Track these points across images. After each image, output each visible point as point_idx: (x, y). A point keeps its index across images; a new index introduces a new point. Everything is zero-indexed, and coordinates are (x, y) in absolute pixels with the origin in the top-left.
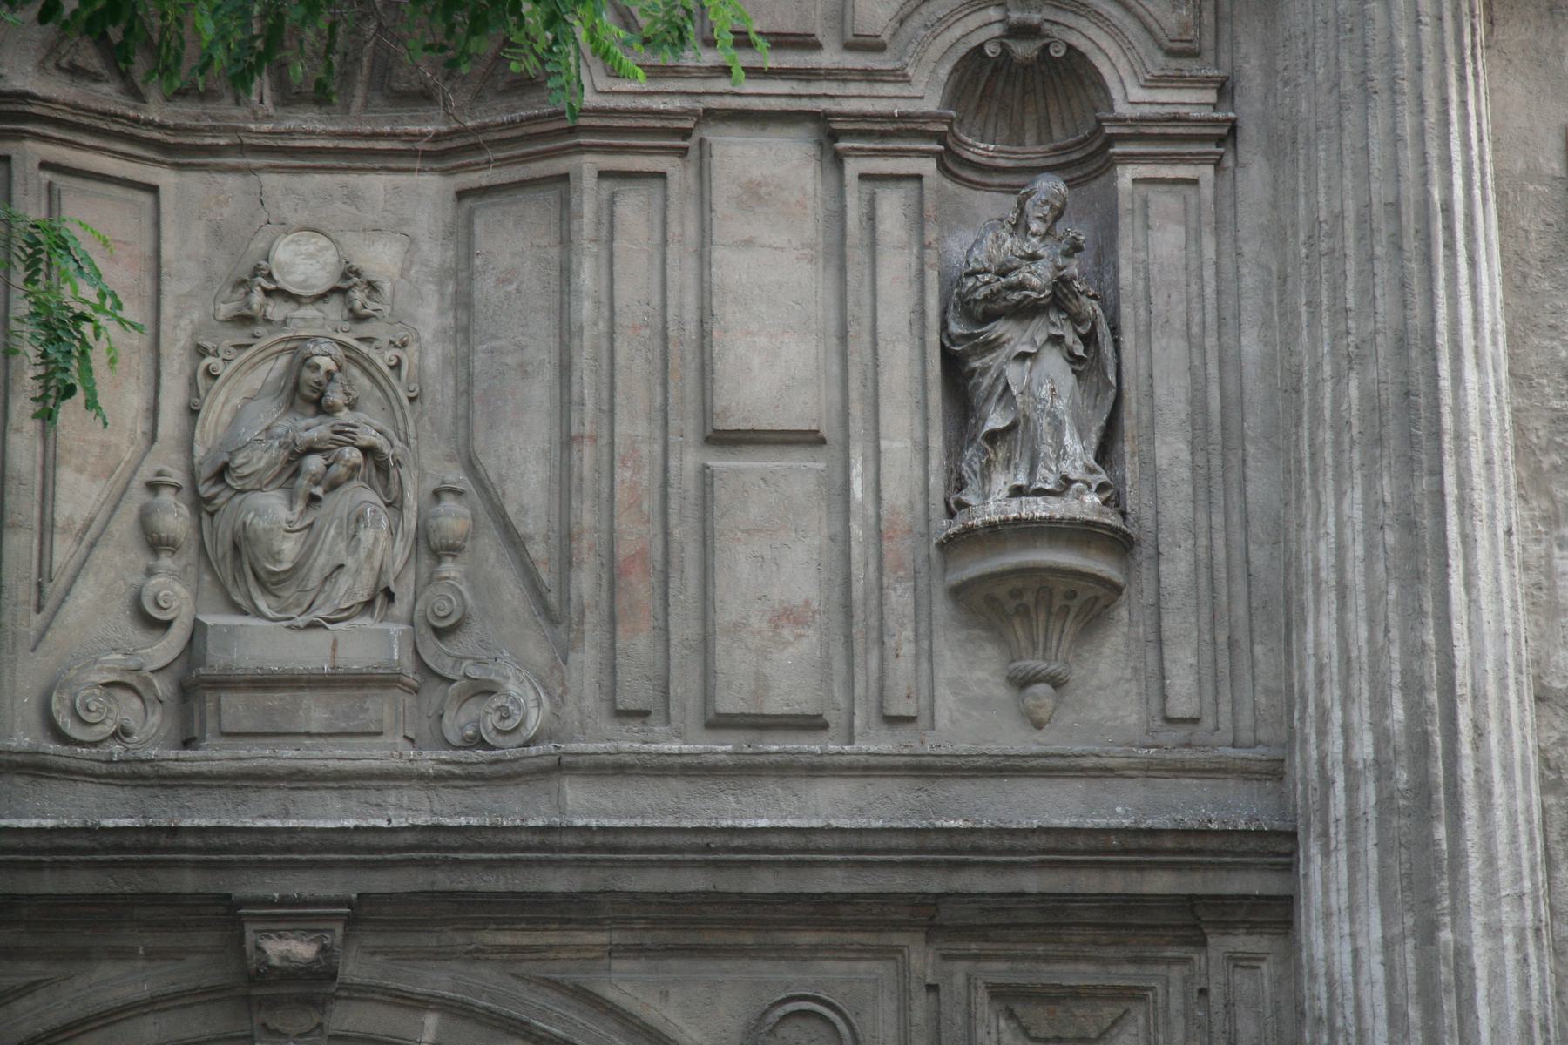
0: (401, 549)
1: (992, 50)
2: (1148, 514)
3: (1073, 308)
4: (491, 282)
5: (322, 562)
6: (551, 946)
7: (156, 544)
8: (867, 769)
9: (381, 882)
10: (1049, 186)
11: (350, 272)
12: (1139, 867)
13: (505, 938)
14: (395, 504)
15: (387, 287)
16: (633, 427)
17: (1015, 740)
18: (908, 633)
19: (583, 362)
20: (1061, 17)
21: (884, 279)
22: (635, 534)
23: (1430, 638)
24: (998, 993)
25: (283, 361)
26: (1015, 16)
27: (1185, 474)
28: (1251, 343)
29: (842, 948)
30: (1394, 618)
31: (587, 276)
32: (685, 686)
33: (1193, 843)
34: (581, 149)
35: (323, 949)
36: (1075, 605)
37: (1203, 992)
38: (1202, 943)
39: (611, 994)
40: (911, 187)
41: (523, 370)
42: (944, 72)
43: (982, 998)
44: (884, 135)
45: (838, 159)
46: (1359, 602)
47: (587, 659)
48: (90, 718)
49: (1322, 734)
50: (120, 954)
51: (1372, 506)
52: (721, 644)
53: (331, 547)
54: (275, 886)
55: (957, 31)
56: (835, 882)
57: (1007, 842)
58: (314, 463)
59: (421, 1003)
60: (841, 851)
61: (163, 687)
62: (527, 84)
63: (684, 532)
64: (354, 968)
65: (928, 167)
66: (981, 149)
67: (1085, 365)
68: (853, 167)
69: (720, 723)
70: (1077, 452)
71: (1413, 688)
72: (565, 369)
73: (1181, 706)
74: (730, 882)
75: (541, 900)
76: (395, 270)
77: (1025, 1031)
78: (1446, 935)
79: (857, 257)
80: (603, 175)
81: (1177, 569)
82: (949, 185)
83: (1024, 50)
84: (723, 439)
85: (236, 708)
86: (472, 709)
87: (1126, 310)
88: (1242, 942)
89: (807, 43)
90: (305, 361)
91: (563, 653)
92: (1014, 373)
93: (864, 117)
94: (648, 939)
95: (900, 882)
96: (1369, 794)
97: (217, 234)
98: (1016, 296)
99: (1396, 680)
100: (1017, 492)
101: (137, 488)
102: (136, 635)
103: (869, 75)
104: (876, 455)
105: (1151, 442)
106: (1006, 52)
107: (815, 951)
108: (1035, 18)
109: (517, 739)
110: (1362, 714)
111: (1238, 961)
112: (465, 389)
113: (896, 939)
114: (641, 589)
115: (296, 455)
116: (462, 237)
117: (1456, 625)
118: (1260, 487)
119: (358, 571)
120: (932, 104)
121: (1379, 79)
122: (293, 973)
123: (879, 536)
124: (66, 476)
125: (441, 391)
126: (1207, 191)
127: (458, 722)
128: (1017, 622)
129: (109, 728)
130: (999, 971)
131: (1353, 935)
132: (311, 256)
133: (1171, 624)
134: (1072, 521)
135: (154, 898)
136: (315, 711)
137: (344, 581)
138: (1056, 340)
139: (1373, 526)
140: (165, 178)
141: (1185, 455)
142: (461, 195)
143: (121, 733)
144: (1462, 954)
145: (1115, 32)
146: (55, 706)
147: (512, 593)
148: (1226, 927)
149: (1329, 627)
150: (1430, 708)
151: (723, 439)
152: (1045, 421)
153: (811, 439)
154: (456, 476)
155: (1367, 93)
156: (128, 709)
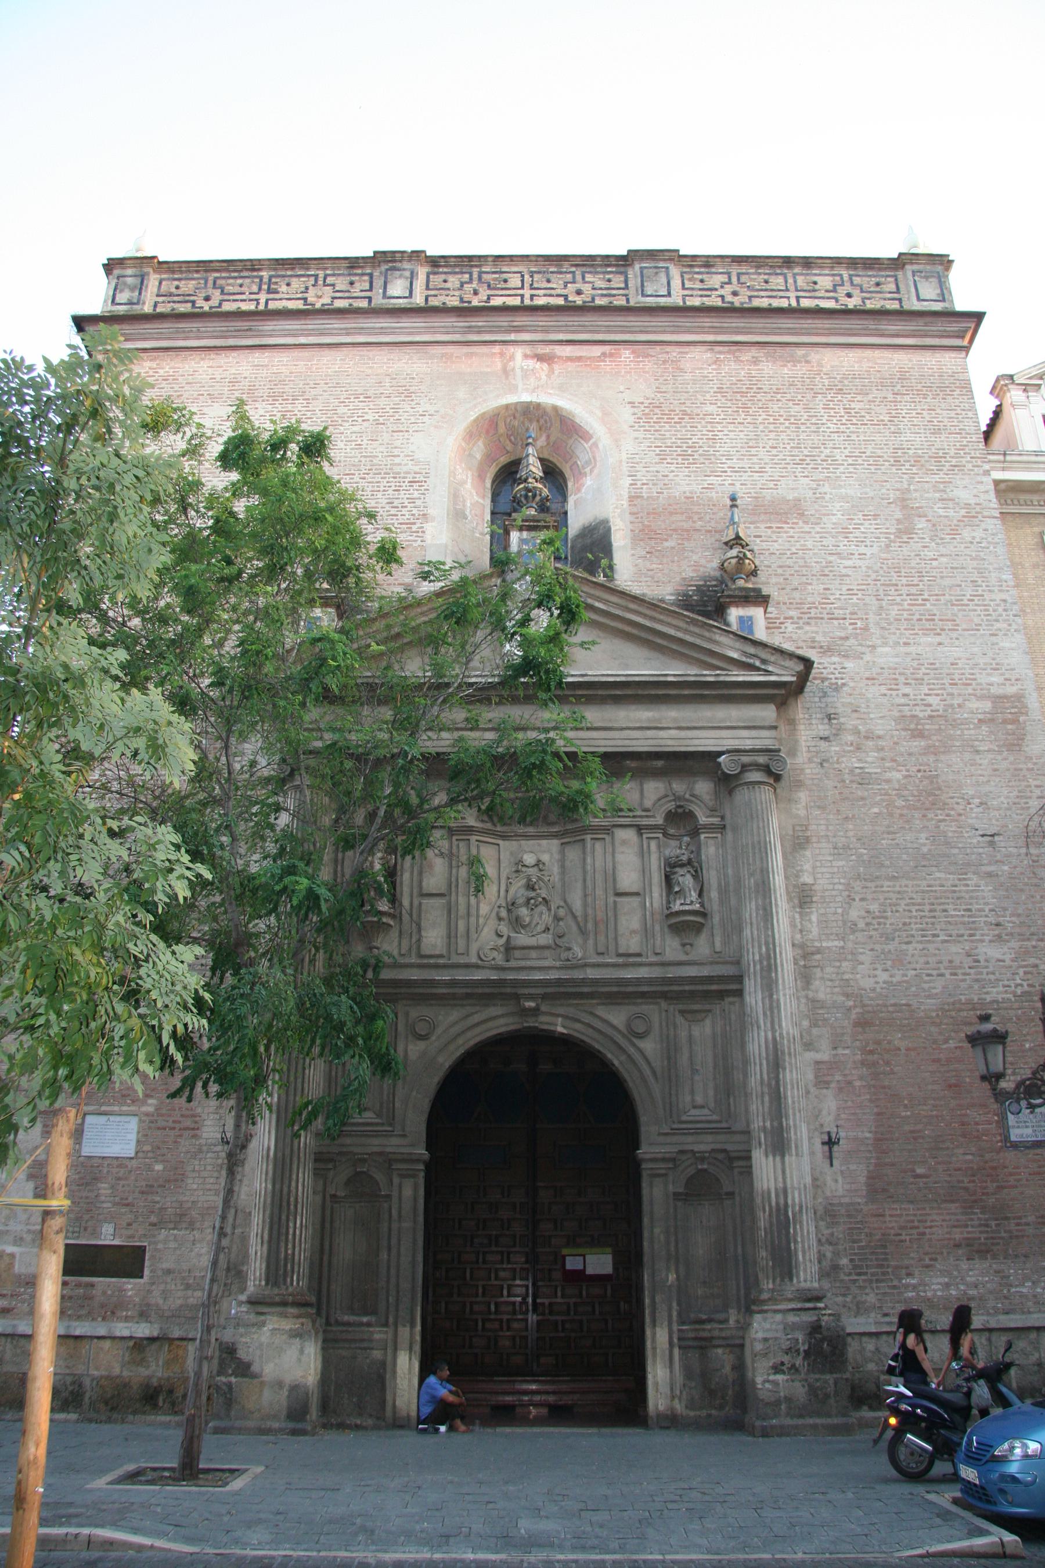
7: (500, 919)
8: (651, 964)
9: (549, 990)
10: (686, 839)
14: (549, 910)
16: (599, 892)
17: (683, 958)
19: (588, 878)
22: (600, 915)
31: (589, 860)
32: (612, 948)
47: (591, 942)
53: (536, 919)
54: (526, 991)
56: (645, 989)
59: (558, 1015)
63: (610, 914)
64: (543, 1008)
66: (672, 831)
69: (619, 955)
70: (694, 895)
71: (767, 944)
72: (585, 880)
74: (623, 989)
79: (646, 855)
81: (716, 920)
83: (680, 810)
85: (517, 954)
88: (731, 999)
90: (529, 880)
91: (585, 941)
92: (680, 879)
96: (758, 967)
97: (512, 854)
102: (495, 937)
104: (651, 897)
110: (756, 950)
111: (731, 1003)
112: (563, 885)
114: (602, 927)
115: (529, 900)
116: (562, 853)
118: (733, 902)
122: (530, 1009)
123: (652, 914)
124: (482, 905)
125: (558, 885)
127: (564, 955)
130: (681, 1007)
135: (501, 994)
136: (534, 954)
139: (757, 909)
140: (500, 842)
144: (778, 1000)
147: (574, 928)
153: (637, 894)
154: (562, 904)
156: (495, 954)
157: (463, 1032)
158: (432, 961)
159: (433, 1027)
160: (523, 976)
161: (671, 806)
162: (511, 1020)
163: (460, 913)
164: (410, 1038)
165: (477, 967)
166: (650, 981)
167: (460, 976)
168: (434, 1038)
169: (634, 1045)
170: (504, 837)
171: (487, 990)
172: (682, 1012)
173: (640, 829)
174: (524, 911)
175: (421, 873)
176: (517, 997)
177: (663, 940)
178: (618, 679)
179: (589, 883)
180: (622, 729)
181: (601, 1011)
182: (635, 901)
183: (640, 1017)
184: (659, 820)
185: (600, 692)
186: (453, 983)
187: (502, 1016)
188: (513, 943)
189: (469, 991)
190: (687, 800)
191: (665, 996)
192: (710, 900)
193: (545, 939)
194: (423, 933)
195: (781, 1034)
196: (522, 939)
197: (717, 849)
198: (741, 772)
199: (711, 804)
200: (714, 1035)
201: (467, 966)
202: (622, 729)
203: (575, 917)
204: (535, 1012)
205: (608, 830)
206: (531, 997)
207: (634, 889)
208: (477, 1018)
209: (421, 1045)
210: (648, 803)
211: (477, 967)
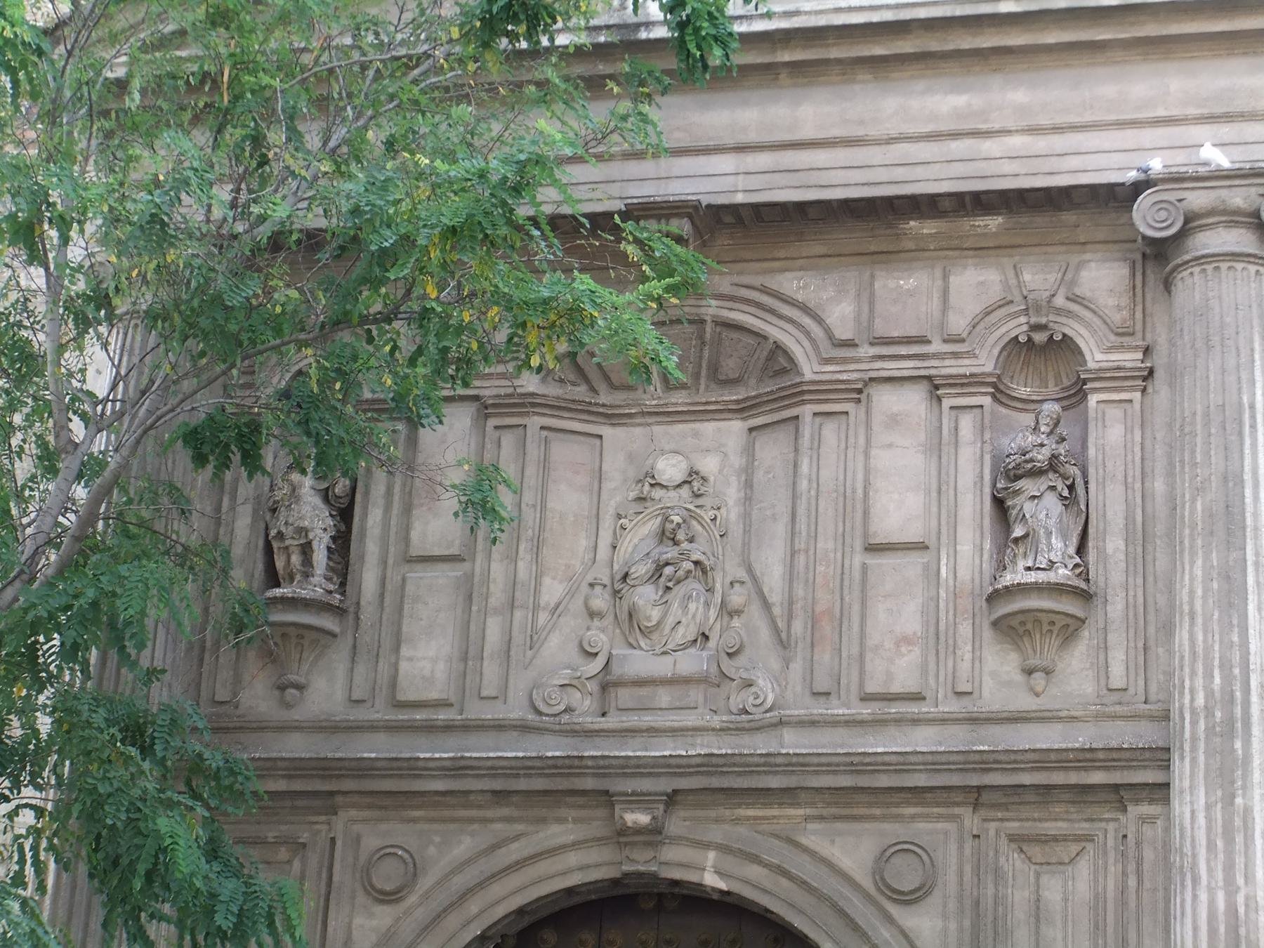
0: (713, 613)
1: (1023, 339)
2: (1101, 580)
3: (1061, 470)
4: (761, 473)
5: (671, 620)
6: (774, 817)
7: (592, 614)
8: (943, 721)
11: (693, 472)
12: (1085, 769)
13: (751, 812)
14: (710, 590)
15: (712, 479)
16: (826, 544)
17: (1025, 702)
18: (969, 647)
19: (801, 510)
20: (1059, 319)
21: (961, 461)
22: (824, 600)
23: (1235, 639)
24: (1012, 838)
25: (659, 519)
26: (1033, 320)
27: (1122, 557)
28: (1159, 486)
29: (928, 816)
30: (1216, 628)
31: (804, 467)
32: (850, 678)
33: (1115, 755)
34: (803, 402)
35: (654, 818)
36: (1056, 629)
37: (1125, 836)
38: (1124, 810)
39: (804, 841)
40: (978, 411)
41: (774, 518)
42: (996, 352)
43: (1004, 842)
44: (962, 385)
45: (939, 399)
46: (1199, 621)
47: (797, 666)
48: (553, 702)
49: (1182, 694)
50: (561, 820)
51: (1207, 568)
52: (869, 656)
53: (675, 611)
54: (629, 785)
55: (1003, 330)
56: (920, 780)
57: (1013, 757)
58: (668, 570)
59: (707, 846)
60: (924, 764)
61: (592, 686)
62: (784, 371)
63: (853, 597)
65: (987, 401)
66: (1023, 391)
67: (1069, 499)
68: (947, 403)
69: (866, 698)
70: (1058, 547)
71: (1226, 666)
73: (1117, 682)
74: (864, 781)
75: (768, 791)
76: (716, 470)
77: (1029, 859)
78: (1239, 801)
81: (1116, 608)
82: (1004, 411)
83: (1040, 338)
84: (874, 548)
85: (624, 696)
86: (743, 694)
87: (1091, 471)
88: (1146, 809)
89: (923, 340)
90: (666, 519)
91: (787, 663)
92: (1029, 508)
93: (951, 376)
94: (825, 812)
95: (955, 780)
98: (1029, 466)
99: (1216, 662)
100: (1029, 569)
101: (585, 588)
102: (577, 658)
103: (955, 355)
105: (1104, 541)
106: (1030, 339)
107: (913, 817)
108: (1043, 320)
109: (762, 709)
111: (1144, 820)
112: (747, 531)
113: (957, 810)
114: (827, 628)
115: (660, 567)
116: (749, 451)
117: (1251, 631)
118: (1162, 561)
119: (688, 625)
120: (989, 368)
121: (1216, 340)
122: (639, 830)
124: (547, 581)
125: (736, 531)
126: (1137, 406)
127: (736, 701)
128: (1025, 639)
129: (562, 707)
131: (1192, 803)
132: (674, 466)
133: (1112, 638)
134: (1049, 583)
136: (664, 697)
138: (1053, 488)
139: (1208, 579)
140: (606, 431)
141: (1123, 547)
142: (751, 430)
143: (569, 710)
144: (1248, 811)
145: (1088, 326)
146: (535, 696)
147: (765, 634)
148: (1137, 801)
149: (1186, 635)
150: (1235, 677)
151: (874, 548)
152: (1042, 531)
153: (922, 547)
154: (742, 574)
155: (1209, 348)
157: (482, 885)
158: (419, 716)
159: (414, 872)
160: (627, 751)
161: (1017, 327)
162: (594, 855)
163: (493, 601)
164: (361, 898)
165: (524, 728)
166: (933, 762)
167: (481, 749)
168: (413, 899)
169: (889, 919)
170: (614, 418)
171: (539, 784)
172: (1017, 840)
173: (934, 386)
174: (645, 596)
175: (408, 510)
176: (606, 798)
177: (977, 659)
178: (876, 17)
179: (802, 525)
180: (891, 141)
181: (814, 838)
182: (912, 564)
183: (905, 849)
184: (986, 362)
185: (835, 53)
186: (458, 768)
187: (575, 845)
188: (617, 670)
189: (497, 785)
190: (1059, 311)
191: (977, 796)
192: (1103, 556)
193: (691, 662)
194: (405, 651)
195: (1250, 901)
196: (639, 662)
197: (1128, 430)
198: (1183, 234)
199: (1117, 318)
200: (1098, 900)
201: (499, 726)
202: (891, 141)
203: (766, 605)
204: (653, 835)
205: (858, 392)
206: (638, 800)
207: (913, 533)
208: (515, 852)
209: (383, 916)
210: (958, 324)
211: (524, 728)
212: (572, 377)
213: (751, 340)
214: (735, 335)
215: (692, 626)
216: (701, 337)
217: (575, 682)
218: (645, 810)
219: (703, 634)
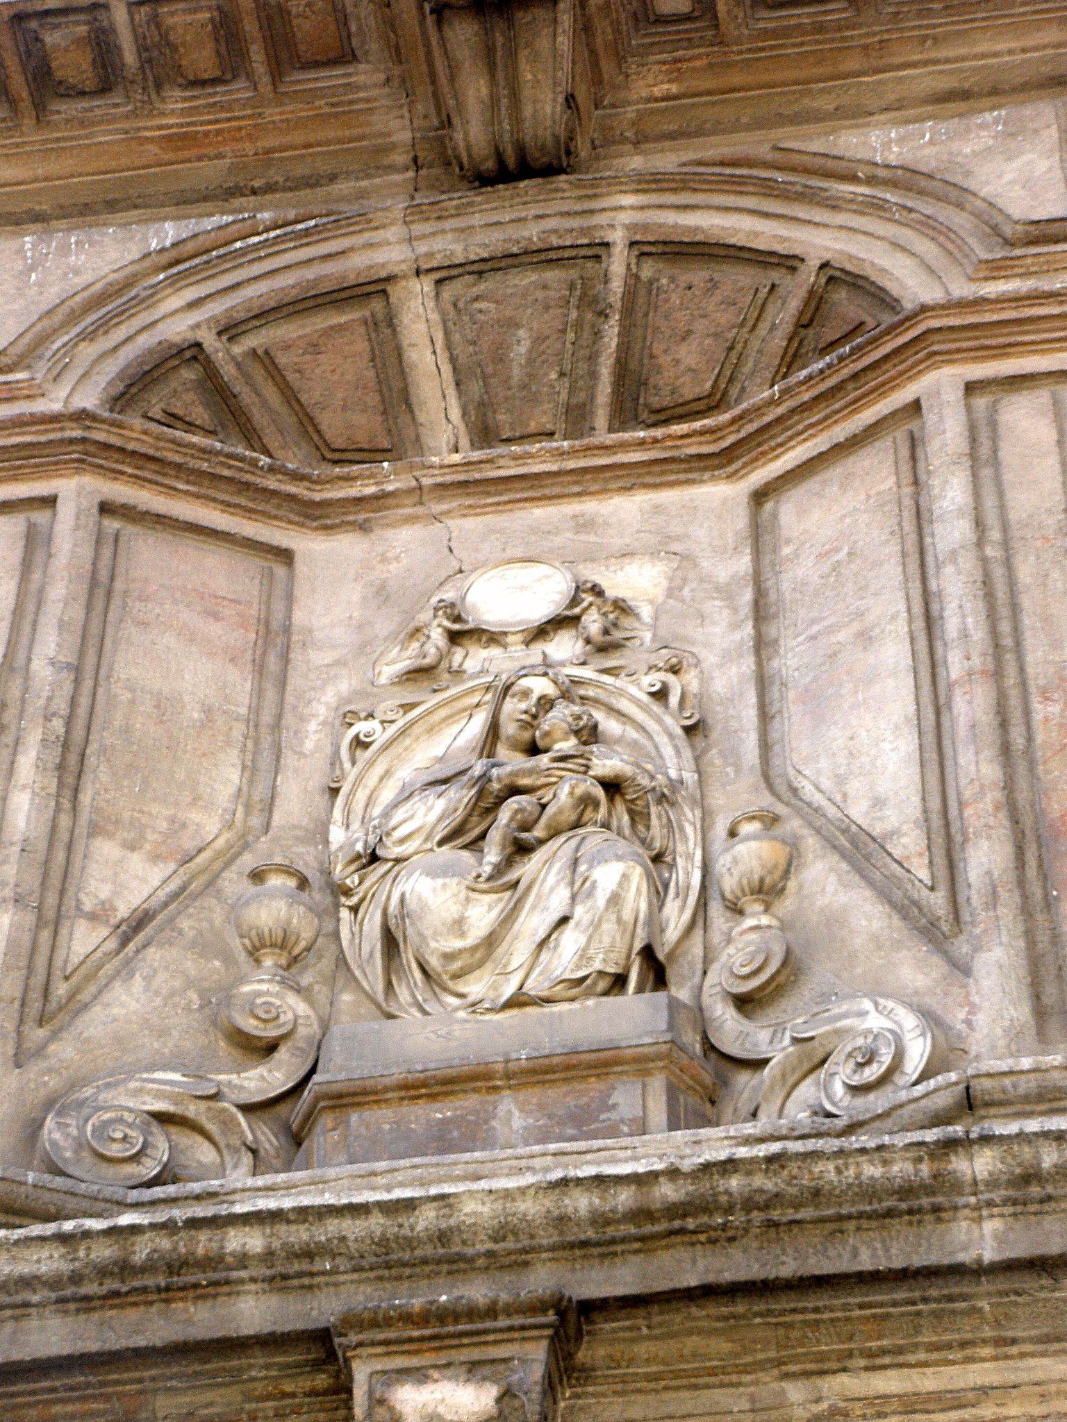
6: (984, 1391)
15: (646, 612)
34: (934, 359)
35: (506, 1395)
41: (865, 638)
48: (115, 1150)
76: (659, 593)
80: (971, 388)
86: (807, 1091)
129: (150, 1169)
137: (571, 940)
212: (200, 414)
213: (743, 278)
214: (697, 275)
215: (609, 927)
216: (592, 304)
217: (192, 1110)
218: (473, 1370)
219: (648, 953)
